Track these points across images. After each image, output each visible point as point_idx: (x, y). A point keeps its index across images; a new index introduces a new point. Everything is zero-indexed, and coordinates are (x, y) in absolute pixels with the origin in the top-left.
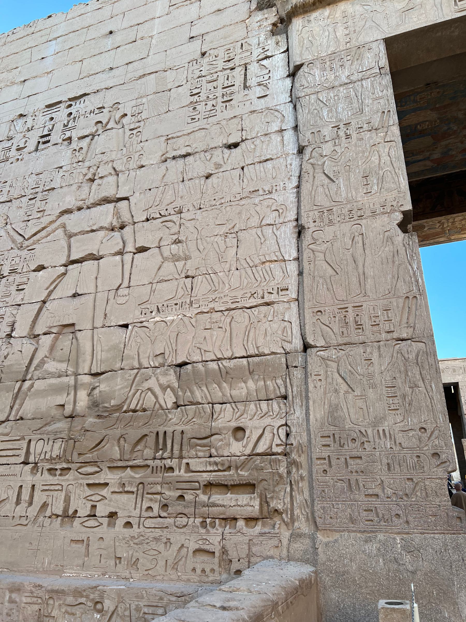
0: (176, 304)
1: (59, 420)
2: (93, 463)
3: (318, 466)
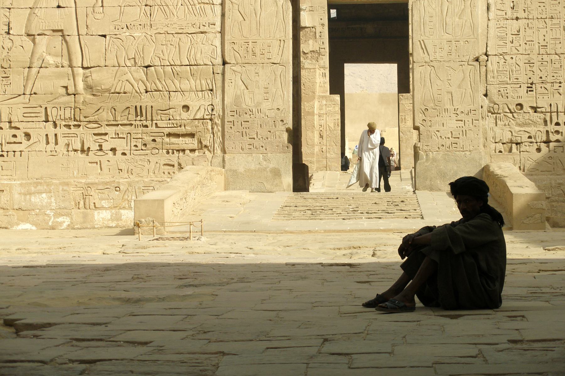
0: (140, 25)
1: (63, 96)
2: (96, 122)
3: (227, 125)
